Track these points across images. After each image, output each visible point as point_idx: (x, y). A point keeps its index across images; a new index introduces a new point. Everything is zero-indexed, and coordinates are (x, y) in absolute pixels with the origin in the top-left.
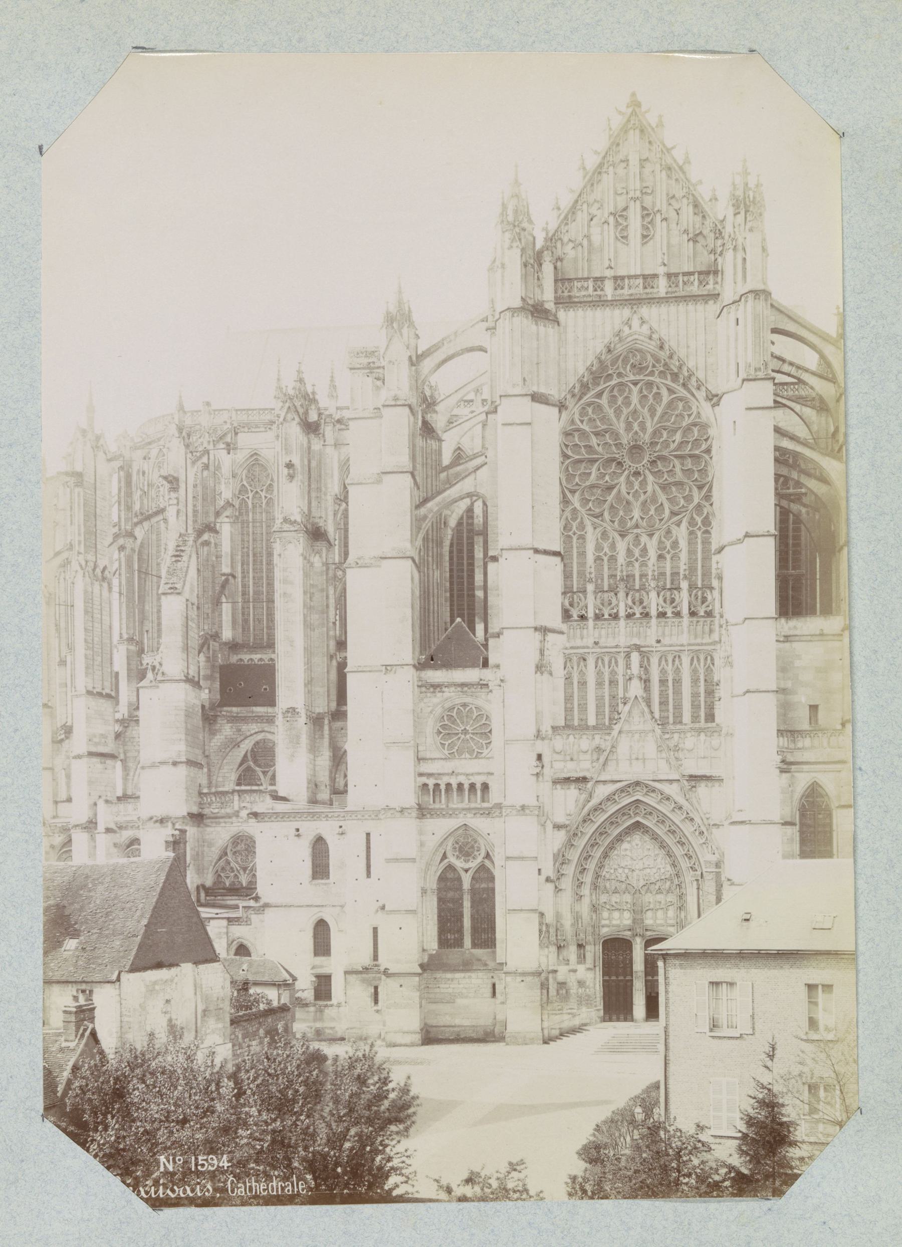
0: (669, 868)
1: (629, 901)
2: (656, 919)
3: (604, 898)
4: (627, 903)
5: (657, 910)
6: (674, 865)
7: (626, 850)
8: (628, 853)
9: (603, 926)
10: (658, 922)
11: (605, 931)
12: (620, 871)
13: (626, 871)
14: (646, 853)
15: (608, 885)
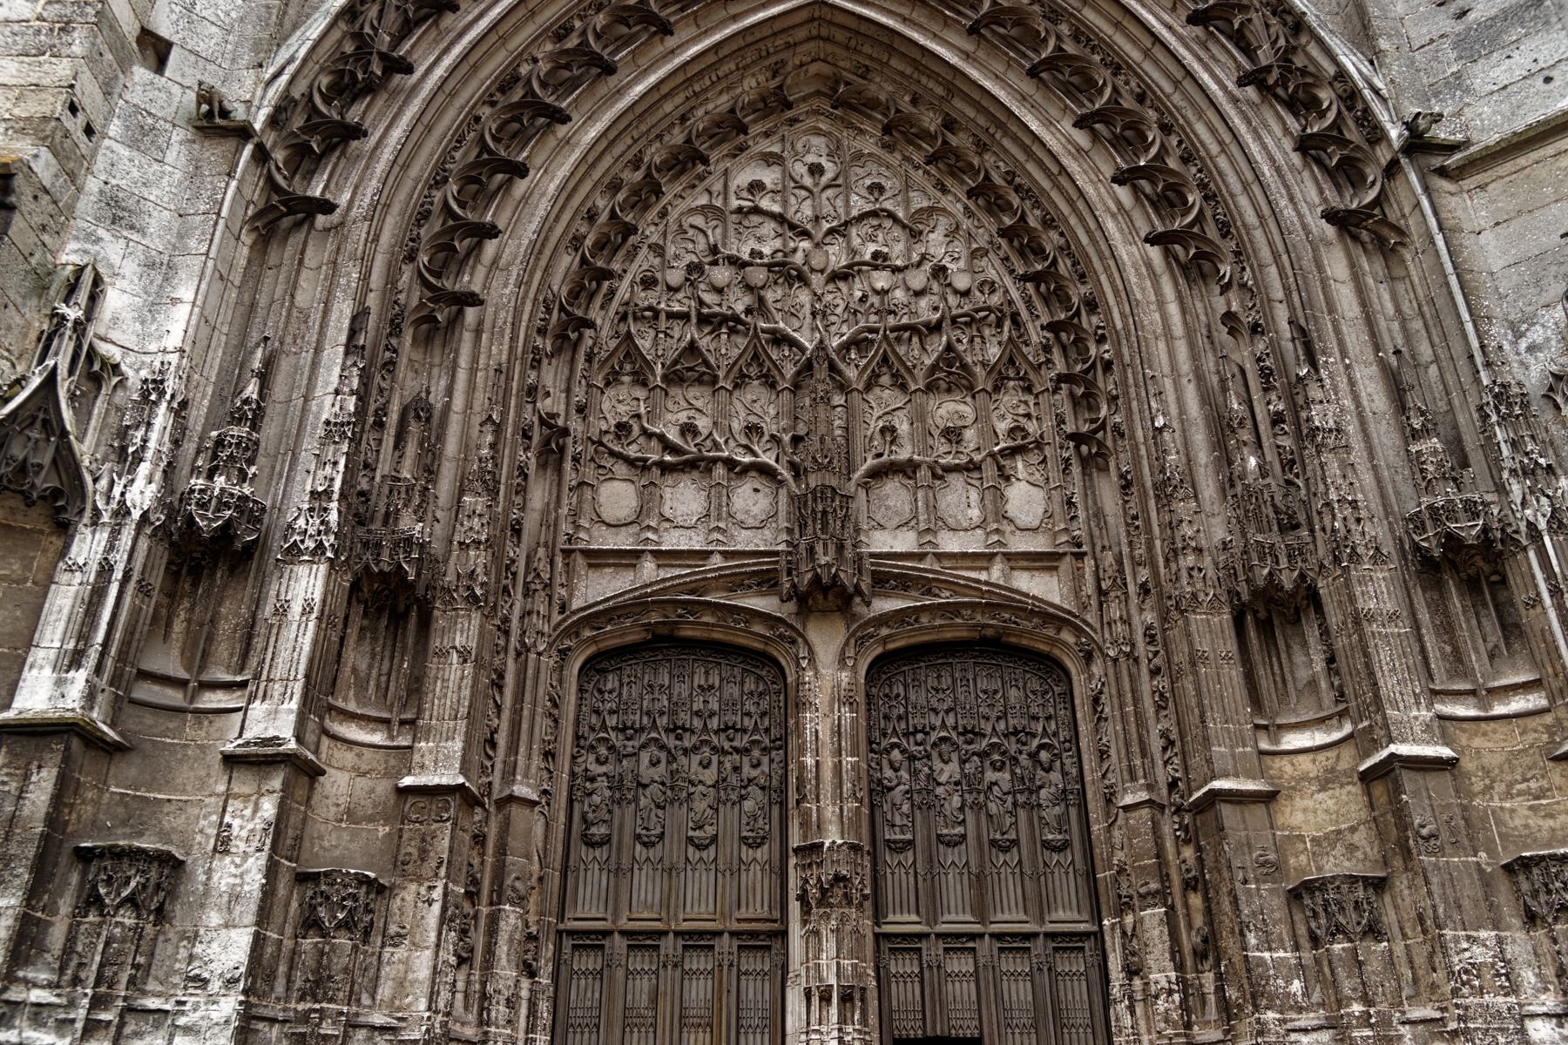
0: (992, 269)
1: (770, 427)
2: (937, 523)
3: (619, 403)
4: (752, 430)
5: (940, 473)
6: (1021, 240)
7: (756, 187)
8: (765, 204)
9: (598, 559)
10: (951, 543)
11: (598, 588)
12: (721, 275)
13: (758, 276)
14: (859, 204)
15: (645, 344)
